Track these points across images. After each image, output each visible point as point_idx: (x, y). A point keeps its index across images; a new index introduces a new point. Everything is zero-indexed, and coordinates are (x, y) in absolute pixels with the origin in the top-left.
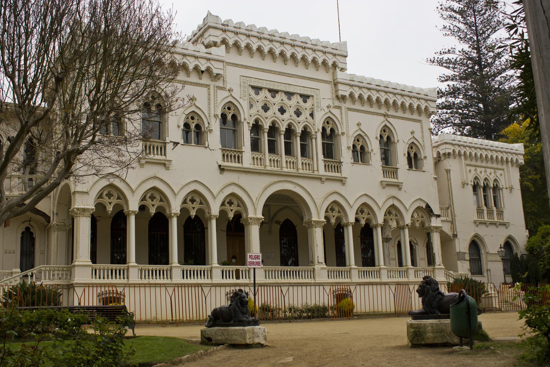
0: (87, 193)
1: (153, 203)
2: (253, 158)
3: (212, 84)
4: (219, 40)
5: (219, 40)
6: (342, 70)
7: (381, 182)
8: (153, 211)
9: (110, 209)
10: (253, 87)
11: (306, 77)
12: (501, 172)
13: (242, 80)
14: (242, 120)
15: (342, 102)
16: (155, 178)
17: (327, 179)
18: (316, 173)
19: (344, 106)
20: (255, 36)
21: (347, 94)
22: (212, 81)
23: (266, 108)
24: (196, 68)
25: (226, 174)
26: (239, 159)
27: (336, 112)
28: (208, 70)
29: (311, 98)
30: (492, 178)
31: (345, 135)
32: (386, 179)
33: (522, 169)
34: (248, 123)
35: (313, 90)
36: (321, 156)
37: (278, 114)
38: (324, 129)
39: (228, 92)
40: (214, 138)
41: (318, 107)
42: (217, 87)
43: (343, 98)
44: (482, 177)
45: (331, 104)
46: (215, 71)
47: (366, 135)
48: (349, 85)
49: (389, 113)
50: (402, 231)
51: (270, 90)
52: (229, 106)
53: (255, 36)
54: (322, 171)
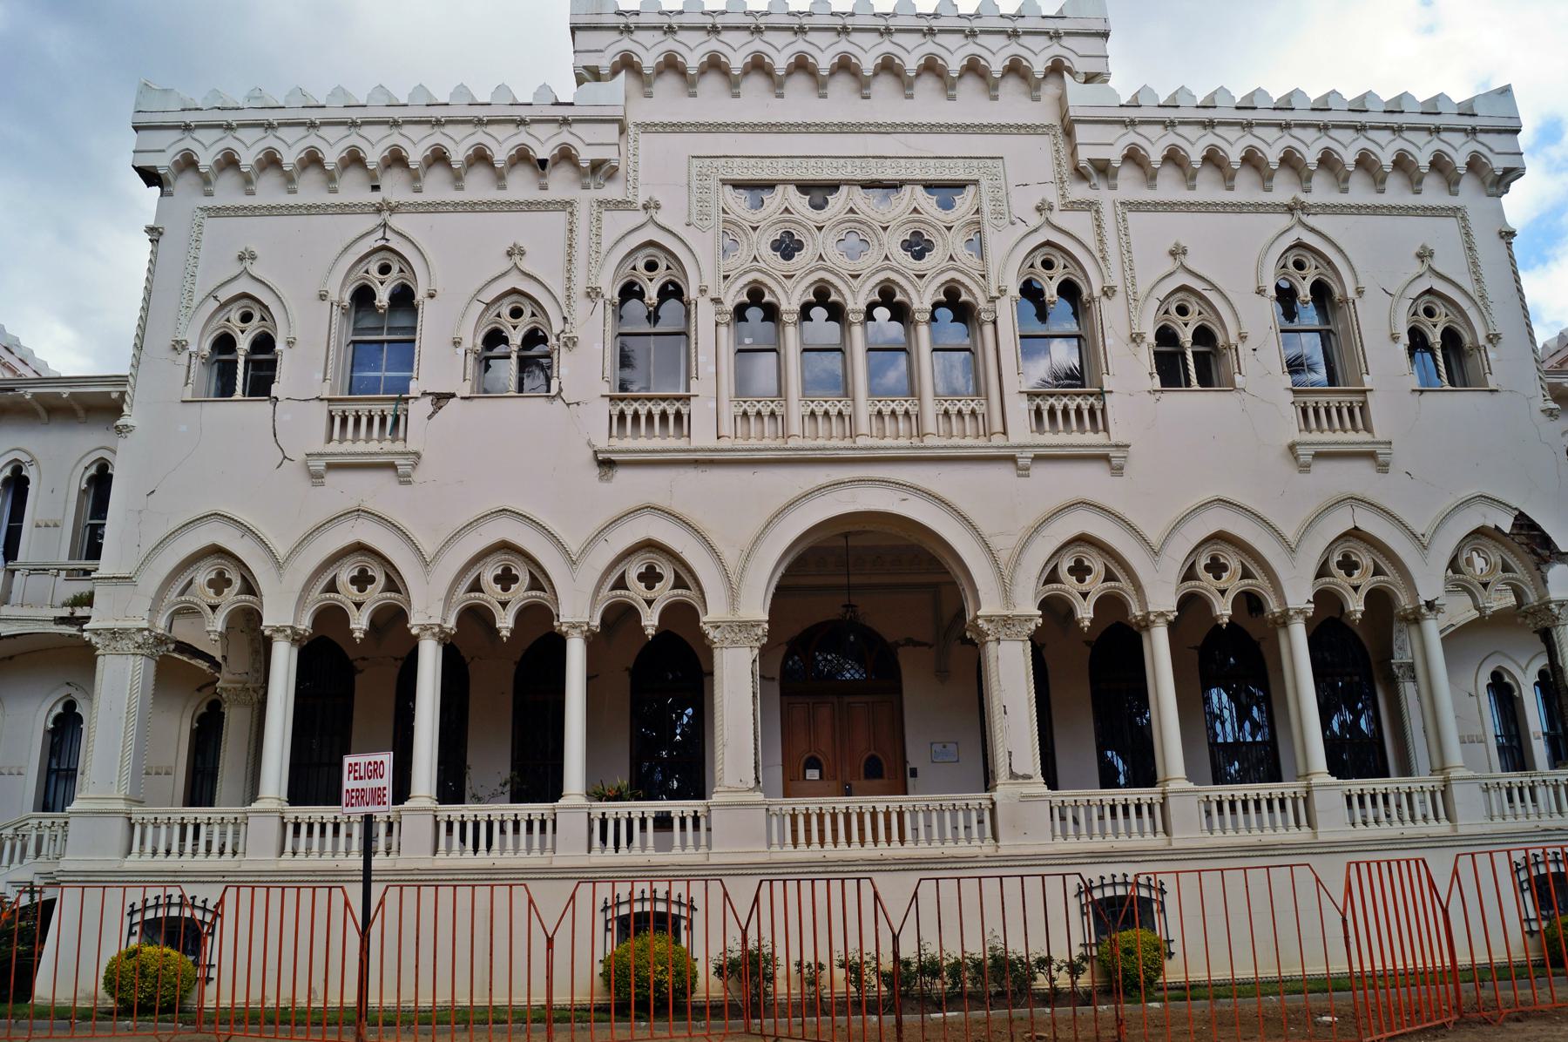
3: (585, 198)
6: (1090, 78)
7: (1292, 447)
10: (737, 185)
11: (949, 126)
13: (694, 171)
15: (1102, 185)
16: (359, 512)
17: (1037, 458)
18: (998, 440)
19: (1104, 196)
20: (737, 28)
22: (586, 187)
24: (522, 156)
25: (621, 475)
27: (1080, 223)
28: (566, 155)
29: (971, 189)
31: (1119, 298)
32: (1306, 437)
34: (717, 301)
35: (975, 162)
39: (643, 212)
40: (585, 365)
41: (999, 215)
42: (600, 203)
43: (1103, 169)
45: (1053, 197)
46: (586, 155)
47: (1214, 287)
48: (1122, 122)
49: (1308, 199)
50: (1413, 629)
51: (804, 187)
52: (653, 255)
53: (737, 28)
54: (1021, 430)
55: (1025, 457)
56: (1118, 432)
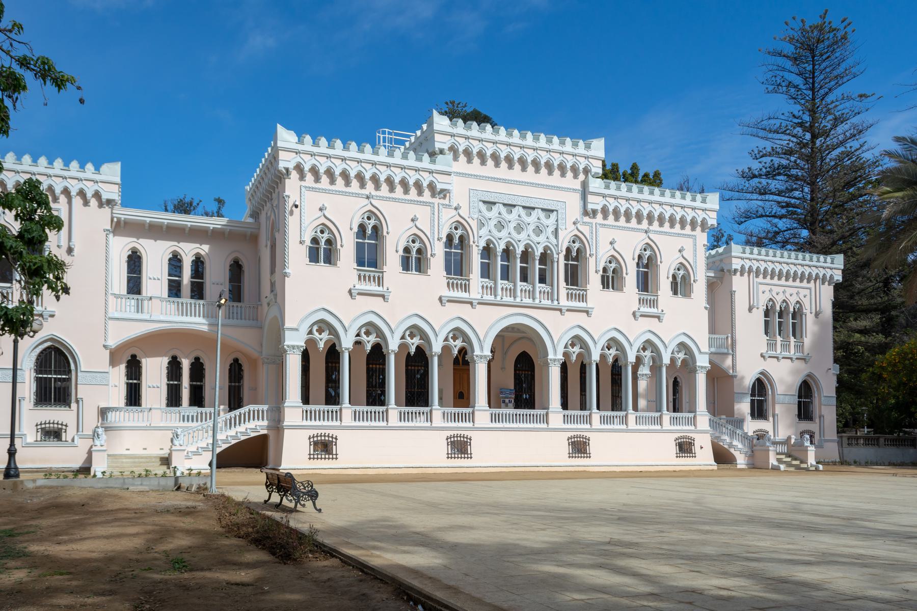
0: (297, 330)
1: (368, 339)
2: (483, 287)
3: (436, 201)
4: (446, 147)
5: (446, 147)
8: (368, 348)
9: (321, 345)
10: (484, 202)
12: (807, 292)
14: (471, 243)
21: (599, 207)
23: (500, 226)
26: (466, 288)
27: (585, 230)
30: (792, 300)
33: (838, 288)
36: (562, 283)
37: (514, 234)
38: (568, 250)
43: (594, 212)
44: (779, 299)
46: (439, 187)
54: (564, 302)
55: (564, 309)
56: (590, 304)
